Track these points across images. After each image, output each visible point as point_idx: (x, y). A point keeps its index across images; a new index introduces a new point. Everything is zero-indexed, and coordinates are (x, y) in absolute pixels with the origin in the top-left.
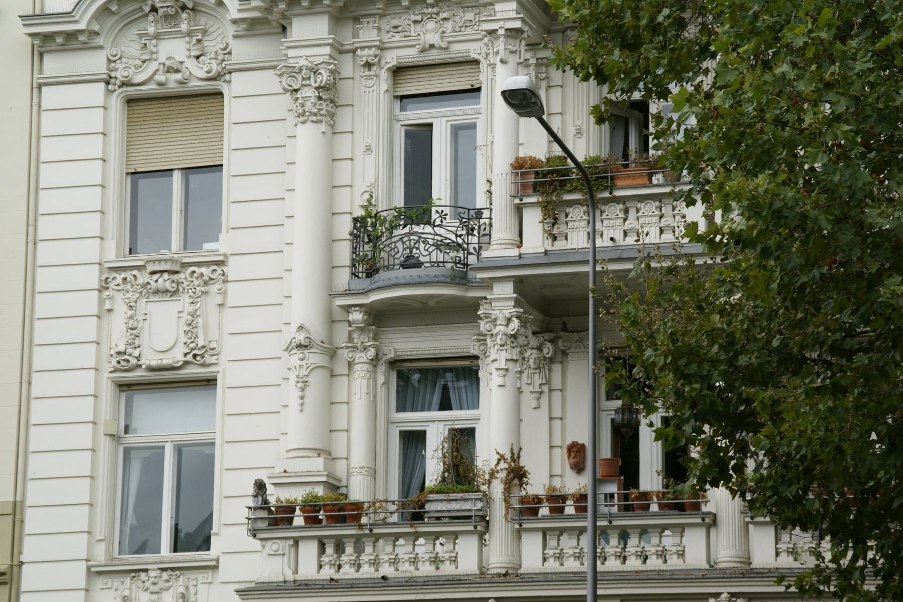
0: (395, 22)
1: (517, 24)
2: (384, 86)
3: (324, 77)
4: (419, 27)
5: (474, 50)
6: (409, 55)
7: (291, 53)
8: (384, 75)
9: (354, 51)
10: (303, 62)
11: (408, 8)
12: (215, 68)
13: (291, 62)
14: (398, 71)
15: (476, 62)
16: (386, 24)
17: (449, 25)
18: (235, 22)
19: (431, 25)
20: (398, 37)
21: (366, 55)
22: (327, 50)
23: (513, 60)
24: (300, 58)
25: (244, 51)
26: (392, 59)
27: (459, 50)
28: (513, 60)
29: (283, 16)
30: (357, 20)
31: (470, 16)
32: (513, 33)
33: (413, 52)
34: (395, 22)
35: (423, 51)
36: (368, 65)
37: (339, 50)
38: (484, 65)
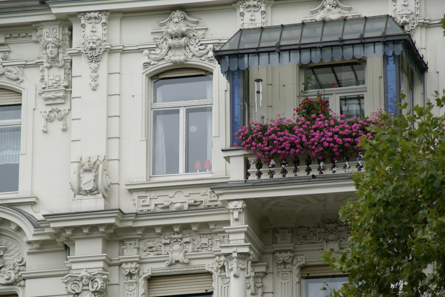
0: (150, 244)
1: (246, 250)
2: (142, 290)
3: (99, 284)
4: (168, 248)
5: (209, 265)
6: (161, 268)
7: (74, 266)
8: (142, 282)
9: (120, 265)
10: (83, 273)
11: (160, 234)
12: (13, 276)
13: (74, 273)
14: (152, 280)
15: (210, 274)
16: (143, 245)
17: (189, 247)
18: (29, 243)
19: (176, 247)
20: (152, 255)
21: (129, 267)
22: (101, 264)
23: (243, 275)
24: (81, 270)
25: (35, 264)
26: (147, 270)
27: (197, 265)
28: (243, 275)
29: (68, 239)
30: (122, 242)
31: (205, 240)
32: (242, 256)
33: (163, 266)
34: (150, 244)
35: (170, 265)
36: (130, 275)
37: (109, 264)
38: (215, 276)
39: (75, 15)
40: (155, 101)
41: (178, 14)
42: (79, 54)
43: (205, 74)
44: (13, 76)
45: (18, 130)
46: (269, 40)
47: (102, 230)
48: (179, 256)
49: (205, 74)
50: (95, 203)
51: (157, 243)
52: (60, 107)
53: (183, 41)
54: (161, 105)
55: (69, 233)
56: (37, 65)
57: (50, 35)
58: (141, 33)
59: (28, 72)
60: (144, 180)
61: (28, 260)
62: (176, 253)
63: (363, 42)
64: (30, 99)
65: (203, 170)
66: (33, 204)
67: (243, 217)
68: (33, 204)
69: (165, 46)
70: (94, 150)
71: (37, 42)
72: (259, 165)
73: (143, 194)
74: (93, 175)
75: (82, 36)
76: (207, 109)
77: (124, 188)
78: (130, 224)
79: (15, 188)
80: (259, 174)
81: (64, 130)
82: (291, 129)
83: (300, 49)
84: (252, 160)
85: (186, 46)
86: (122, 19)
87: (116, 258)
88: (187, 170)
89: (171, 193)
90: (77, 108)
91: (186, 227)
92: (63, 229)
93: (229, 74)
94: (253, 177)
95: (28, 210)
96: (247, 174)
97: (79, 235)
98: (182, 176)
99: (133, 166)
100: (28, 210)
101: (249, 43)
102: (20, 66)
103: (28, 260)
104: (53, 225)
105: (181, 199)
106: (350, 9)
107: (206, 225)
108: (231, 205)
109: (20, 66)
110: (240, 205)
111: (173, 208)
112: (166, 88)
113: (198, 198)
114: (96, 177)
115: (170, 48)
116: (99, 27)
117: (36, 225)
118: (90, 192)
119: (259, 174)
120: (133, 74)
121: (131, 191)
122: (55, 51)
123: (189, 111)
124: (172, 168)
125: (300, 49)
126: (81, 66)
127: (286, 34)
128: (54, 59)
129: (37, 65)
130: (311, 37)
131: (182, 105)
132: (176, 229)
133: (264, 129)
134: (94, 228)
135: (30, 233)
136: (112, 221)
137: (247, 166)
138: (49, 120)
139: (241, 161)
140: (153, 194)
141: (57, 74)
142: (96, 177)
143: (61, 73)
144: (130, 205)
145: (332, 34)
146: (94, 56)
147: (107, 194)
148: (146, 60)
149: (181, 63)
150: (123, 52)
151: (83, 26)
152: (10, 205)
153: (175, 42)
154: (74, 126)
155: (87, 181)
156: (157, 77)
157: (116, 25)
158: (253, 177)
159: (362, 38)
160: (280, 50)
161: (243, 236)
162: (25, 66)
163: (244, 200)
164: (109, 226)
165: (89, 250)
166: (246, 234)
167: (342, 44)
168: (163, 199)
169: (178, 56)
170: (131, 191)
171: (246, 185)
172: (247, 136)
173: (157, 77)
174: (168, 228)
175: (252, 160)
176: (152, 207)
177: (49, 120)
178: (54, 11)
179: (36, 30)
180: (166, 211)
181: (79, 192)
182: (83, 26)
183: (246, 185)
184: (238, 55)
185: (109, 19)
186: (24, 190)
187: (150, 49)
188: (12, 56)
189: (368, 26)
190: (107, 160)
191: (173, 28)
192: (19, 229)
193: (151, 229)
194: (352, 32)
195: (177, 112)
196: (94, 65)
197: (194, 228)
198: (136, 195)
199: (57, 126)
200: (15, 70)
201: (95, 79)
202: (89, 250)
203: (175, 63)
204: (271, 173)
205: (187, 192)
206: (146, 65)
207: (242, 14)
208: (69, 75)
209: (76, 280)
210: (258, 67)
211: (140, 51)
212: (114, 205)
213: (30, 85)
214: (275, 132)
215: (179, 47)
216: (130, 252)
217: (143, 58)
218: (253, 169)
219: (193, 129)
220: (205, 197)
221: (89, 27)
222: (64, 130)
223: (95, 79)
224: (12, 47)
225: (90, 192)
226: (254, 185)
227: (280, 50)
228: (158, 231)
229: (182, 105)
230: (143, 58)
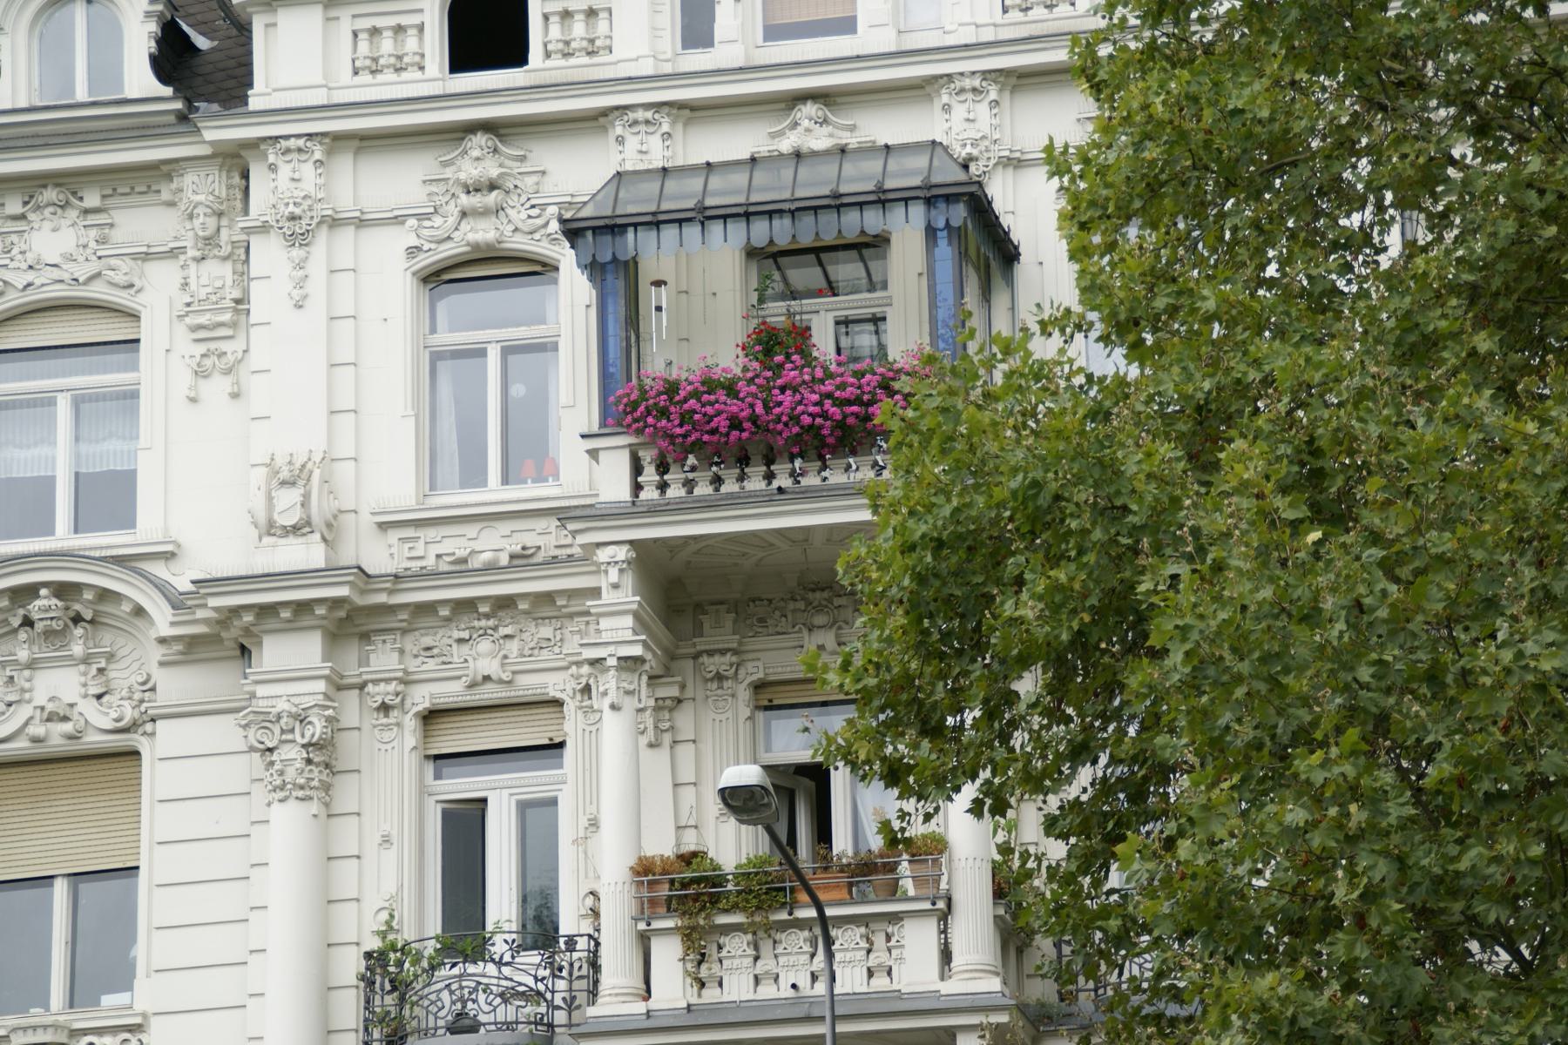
0: (427, 641)
1: (637, 651)
3: (317, 728)
4: (465, 649)
5: (556, 685)
6: (451, 692)
7: (261, 691)
8: (411, 723)
9: (362, 687)
10: (282, 705)
11: (448, 620)
12: (129, 714)
13: (261, 705)
14: (431, 717)
15: (558, 703)
16: (411, 644)
17: (513, 647)
18: (163, 641)
19: (485, 645)
20: (431, 664)
21: (381, 692)
22: (321, 686)
23: (630, 704)
24: (278, 698)
25: (176, 686)
26: (422, 697)
28: (630, 704)
30: (365, 637)
31: (546, 631)
34: (427, 641)
36: (385, 708)
37: (338, 685)
39: (254, 144)
40: (433, 330)
41: (480, 139)
42: (264, 228)
43: (542, 269)
44: (120, 278)
45: (134, 395)
46: (682, 194)
47: (320, 611)
48: (490, 666)
49: (542, 269)
50: (307, 553)
51: (441, 639)
52: (224, 346)
53: (493, 198)
54: (447, 338)
55: (248, 618)
56: (173, 253)
57: (201, 187)
58: (399, 182)
59: (155, 269)
60: (411, 502)
61: (161, 677)
62: (484, 658)
63: (882, 199)
64: (156, 330)
65: (540, 479)
66: (169, 556)
67: (629, 581)
68: (169, 556)
69: (453, 210)
70: (299, 437)
71: (171, 204)
72: (663, 468)
73: (409, 532)
74: (300, 493)
75: (273, 187)
76: (547, 347)
77: (367, 520)
78: (382, 598)
79: (129, 522)
80: (663, 487)
81: (235, 396)
82: (731, 388)
83: (747, 214)
84: (647, 456)
85: (499, 210)
86: (358, 152)
87: (352, 672)
88: (505, 480)
89: (471, 530)
90: (262, 346)
91: (505, 604)
92: (236, 611)
93: (595, 269)
94: (650, 494)
95: (158, 570)
96: (637, 488)
97: (271, 624)
98: (494, 493)
99: (388, 473)
100: (158, 570)
101: (636, 202)
102: (135, 257)
103: (161, 677)
104: (214, 602)
105: (493, 543)
106: (852, 128)
107: (548, 597)
108: (603, 555)
109: (135, 257)
110: (622, 553)
111: (476, 562)
112: (458, 302)
113: (531, 540)
114: (306, 497)
115: (464, 214)
116: (308, 171)
117: (177, 602)
118: (295, 530)
119: (663, 487)
120: (384, 270)
121: (384, 526)
122: (212, 222)
123: (508, 351)
124: (473, 475)
125: (747, 214)
126: (269, 255)
127: (715, 182)
128: (210, 241)
129: (173, 253)
130: (771, 188)
131: (493, 338)
132: (484, 608)
133: (672, 388)
134: (302, 607)
135: (163, 620)
136: (343, 591)
137: (637, 469)
138: (201, 373)
139: (624, 459)
140: (431, 533)
141: (218, 273)
142: (306, 497)
143: (226, 270)
144: (381, 556)
145: (815, 183)
146: (299, 231)
147: (331, 534)
148: (413, 241)
149: (489, 246)
150: (361, 223)
151: (273, 168)
152: (120, 561)
153: (475, 200)
154: (256, 387)
155: (288, 506)
156: (439, 278)
157: (344, 163)
158: (650, 494)
159: (881, 190)
160: (704, 216)
161: (629, 621)
162: (147, 257)
163: (631, 542)
164: (336, 603)
165: (293, 656)
166: (636, 615)
167: (837, 203)
168: (454, 543)
169: (483, 232)
170: (384, 526)
171: (634, 510)
172: (634, 405)
173: (439, 278)
174: (465, 607)
175: (647, 456)
176: (430, 562)
177: (201, 373)
178: (209, 135)
179: (169, 177)
180: (461, 568)
181: (270, 528)
182: (273, 168)
183: (634, 510)
184: (613, 228)
185: (330, 152)
186: (148, 529)
187: (421, 217)
188: (117, 235)
189: (893, 165)
190: (329, 459)
191: (469, 170)
192: (139, 611)
193: (428, 608)
194: (858, 178)
195: (482, 353)
196: (297, 253)
197: (523, 606)
198: (394, 536)
199: (217, 387)
200: (124, 265)
201: (300, 284)
202: (293, 656)
203: (476, 247)
204: (689, 485)
205: (505, 527)
206: (413, 251)
207: (620, 140)
208: (243, 274)
209: (266, 720)
210: (658, 254)
211: (398, 220)
212: (347, 557)
213: (159, 296)
214: (696, 394)
215: (485, 213)
216: (384, 659)
217: (405, 237)
218: (650, 475)
219: (518, 390)
220: (546, 537)
221: (285, 171)
222: (235, 396)
223: (300, 284)
224: (118, 216)
225: (295, 530)
226: (653, 510)
227: (704, 216)
228: (444, 612)
229: (493, 338)
230: (405, 237)
